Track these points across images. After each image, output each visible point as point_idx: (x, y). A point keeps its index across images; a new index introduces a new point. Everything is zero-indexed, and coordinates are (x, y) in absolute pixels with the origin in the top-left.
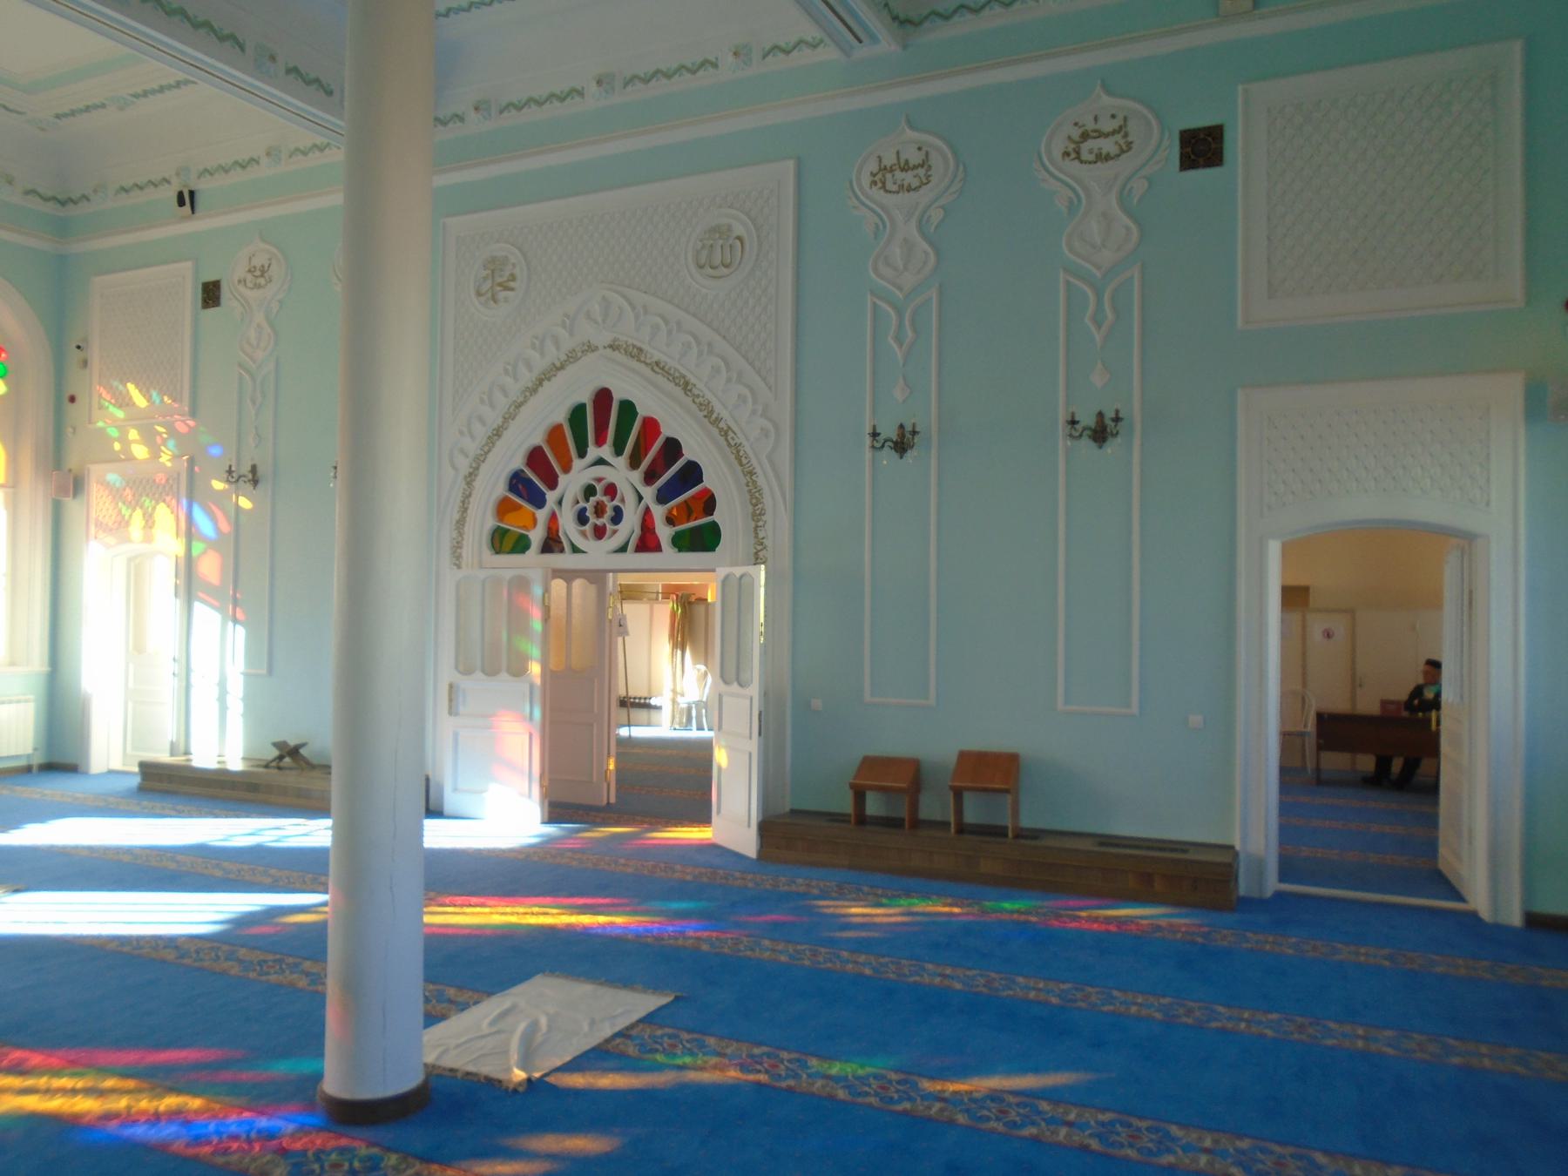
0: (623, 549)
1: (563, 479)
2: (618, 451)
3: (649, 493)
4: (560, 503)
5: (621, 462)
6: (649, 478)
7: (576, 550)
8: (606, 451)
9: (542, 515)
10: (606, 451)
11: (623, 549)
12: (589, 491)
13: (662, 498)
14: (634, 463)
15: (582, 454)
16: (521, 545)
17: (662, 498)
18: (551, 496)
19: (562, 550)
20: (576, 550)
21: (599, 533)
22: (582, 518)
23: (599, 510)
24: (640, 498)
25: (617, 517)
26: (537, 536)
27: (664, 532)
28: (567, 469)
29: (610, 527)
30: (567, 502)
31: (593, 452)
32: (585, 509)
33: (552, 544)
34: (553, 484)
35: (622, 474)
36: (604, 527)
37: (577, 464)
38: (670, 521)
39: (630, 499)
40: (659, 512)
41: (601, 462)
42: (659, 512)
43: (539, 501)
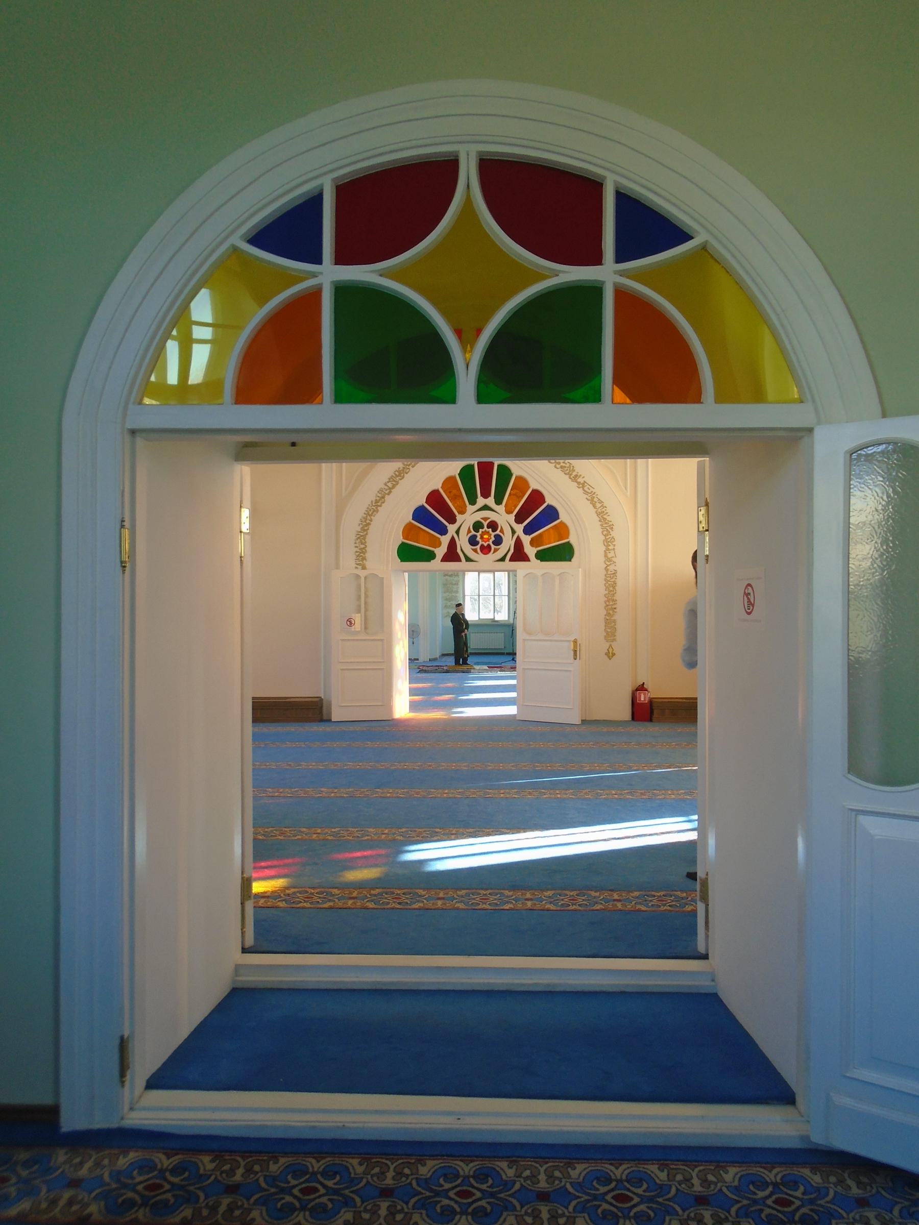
0: (502, 559)
1: (459, 518)
2: (498, 501)
3: (519, 529)
4: (457, 532)
5: (501, 509)
6: (519, 519)
7: (468, 559)
8: (491, 501)
9: (445, 540)
10: (491, 501)
11: (502, 559)
12: (477, 526)
13: (527, 531)
14: (509, 512)
15: (473, 502)
16: (429, 556)
17: (527, 531)
18: (452, 528)
19: (459, 560)
20: (468, 559)
21: (486, 550)
22: (473, 541)
23: (485, 539)
24: (513, 532)
25: (498, 541)
26: (441, 551)
27: (530, 551)
28: (462, 512)
29: (493, 547)
30: (463, 531)
31: (481, 501)
32: (475, 536)
33: (452, 555)
34: (452, 520)
35: (504, 518)
36: (489, 546)
37: (470, 508)
38: (533, 543)
39: (508, 532)
40: (526, 540)
41: (486, 508)
42: (526, 540)
43: (443, 531)
